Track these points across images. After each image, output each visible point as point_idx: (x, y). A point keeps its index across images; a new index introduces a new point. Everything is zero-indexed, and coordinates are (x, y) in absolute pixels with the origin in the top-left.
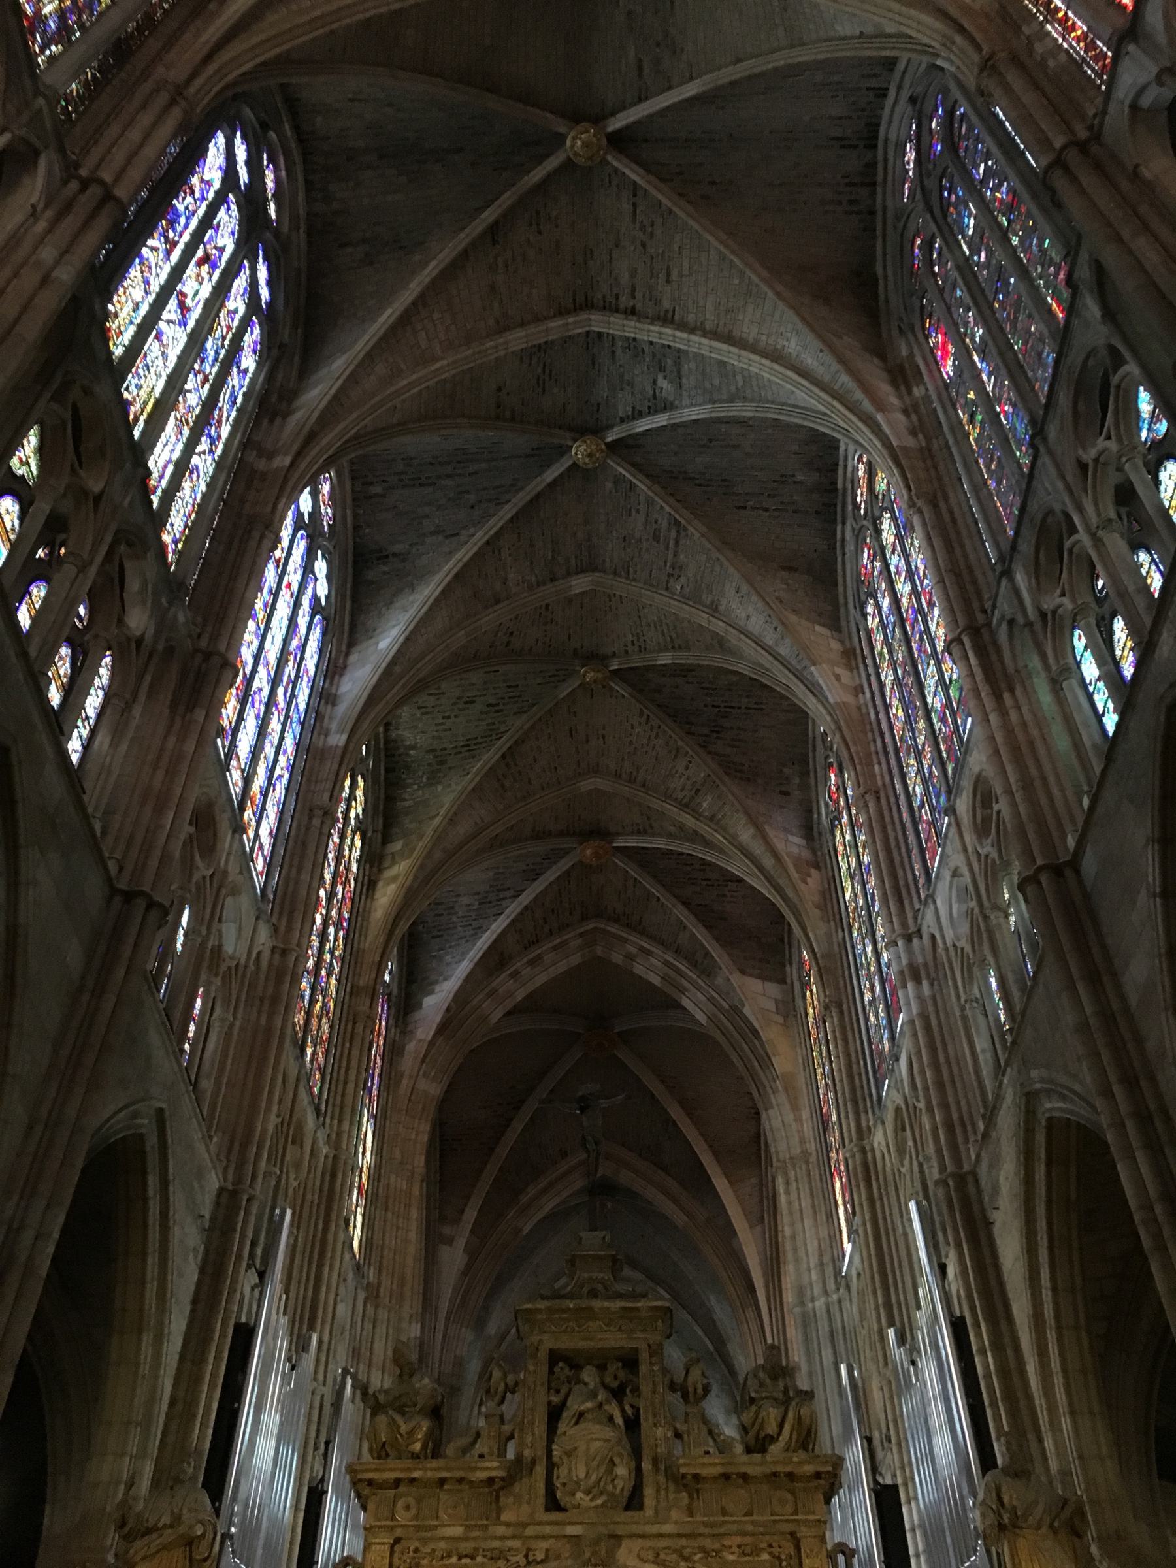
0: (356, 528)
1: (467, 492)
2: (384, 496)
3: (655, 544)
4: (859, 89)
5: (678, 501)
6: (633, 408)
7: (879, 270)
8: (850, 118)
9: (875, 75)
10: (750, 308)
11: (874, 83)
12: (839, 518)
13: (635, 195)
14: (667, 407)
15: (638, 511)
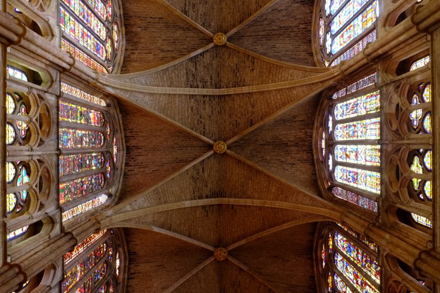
0: (312, 12)
1: (267, 24)
2: (300, 24)
3: (194, 3)
4: (134, 166)
5: (185, 21)
6: (203, 57)
7: (120, 116)
8: (136, 156)
9: (130, 171)
10: (163, 105)
11: (130, 168)
12: (122, 16)
13: (204, 132)
14: (191, 59)
15: (201, 15)
